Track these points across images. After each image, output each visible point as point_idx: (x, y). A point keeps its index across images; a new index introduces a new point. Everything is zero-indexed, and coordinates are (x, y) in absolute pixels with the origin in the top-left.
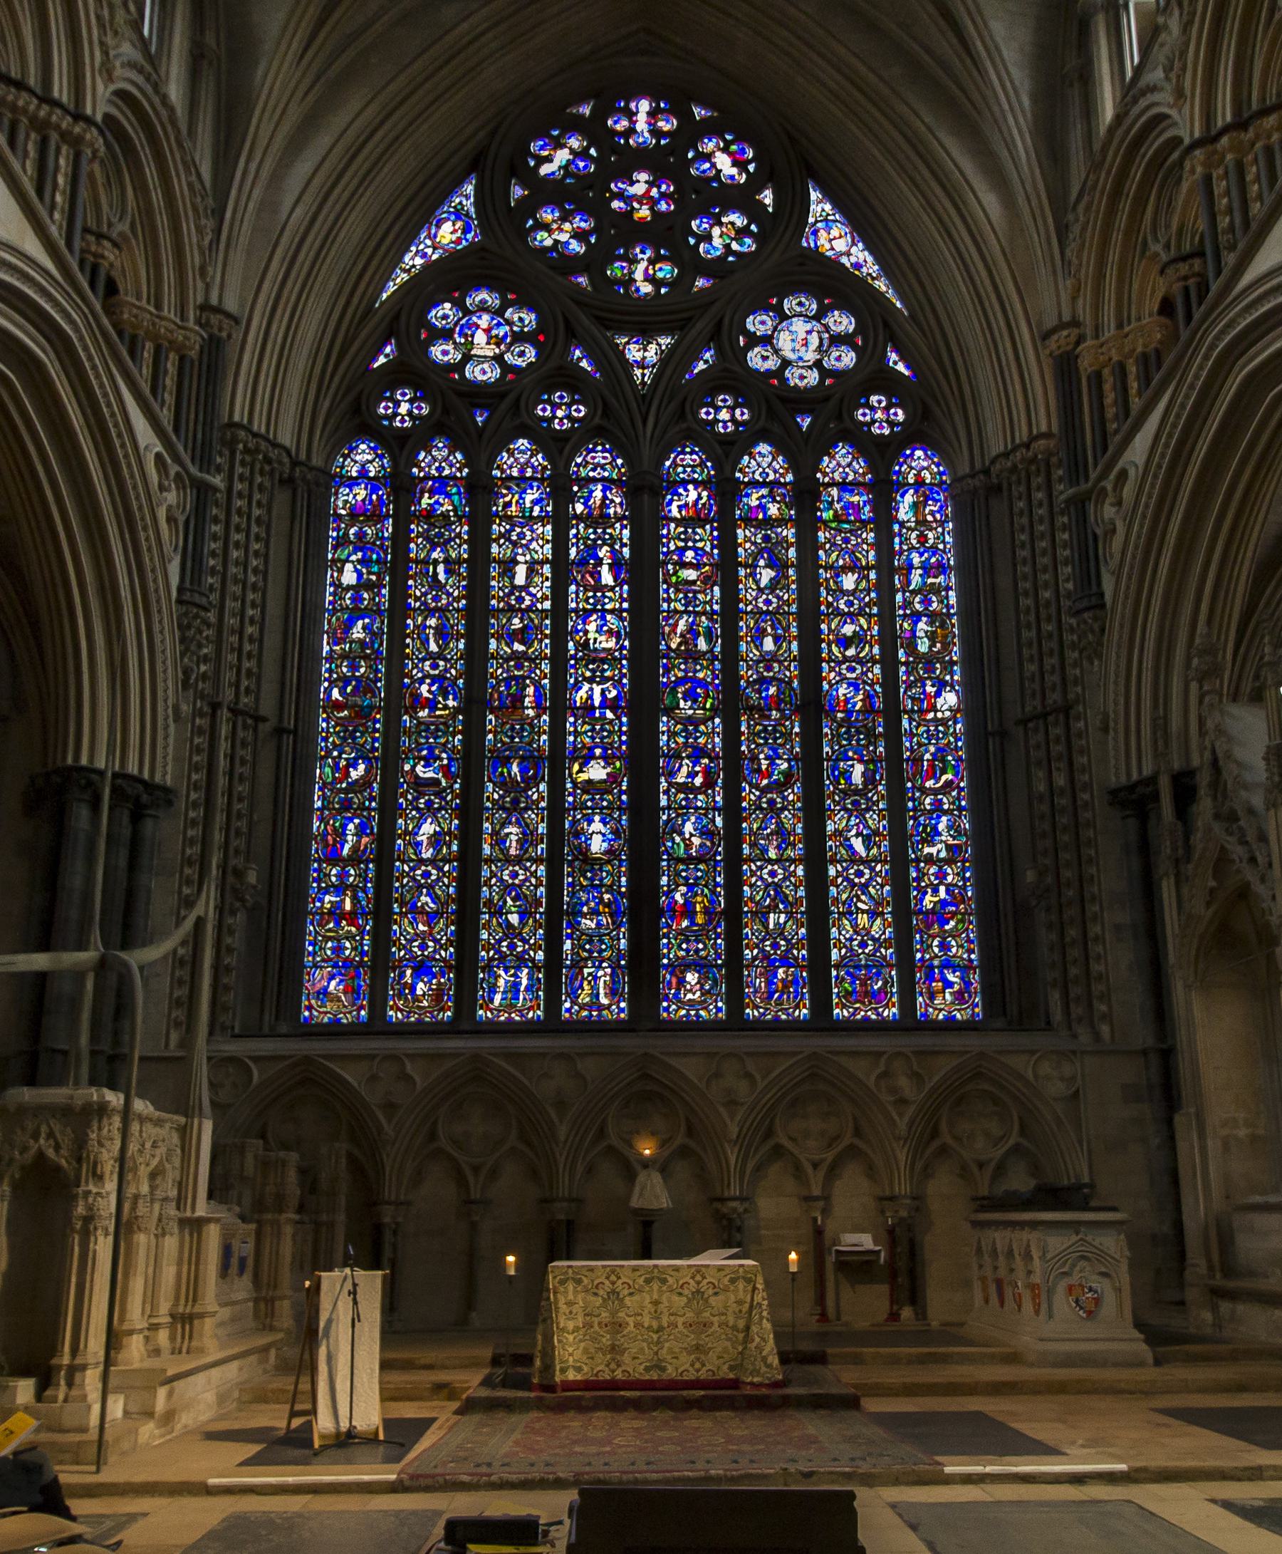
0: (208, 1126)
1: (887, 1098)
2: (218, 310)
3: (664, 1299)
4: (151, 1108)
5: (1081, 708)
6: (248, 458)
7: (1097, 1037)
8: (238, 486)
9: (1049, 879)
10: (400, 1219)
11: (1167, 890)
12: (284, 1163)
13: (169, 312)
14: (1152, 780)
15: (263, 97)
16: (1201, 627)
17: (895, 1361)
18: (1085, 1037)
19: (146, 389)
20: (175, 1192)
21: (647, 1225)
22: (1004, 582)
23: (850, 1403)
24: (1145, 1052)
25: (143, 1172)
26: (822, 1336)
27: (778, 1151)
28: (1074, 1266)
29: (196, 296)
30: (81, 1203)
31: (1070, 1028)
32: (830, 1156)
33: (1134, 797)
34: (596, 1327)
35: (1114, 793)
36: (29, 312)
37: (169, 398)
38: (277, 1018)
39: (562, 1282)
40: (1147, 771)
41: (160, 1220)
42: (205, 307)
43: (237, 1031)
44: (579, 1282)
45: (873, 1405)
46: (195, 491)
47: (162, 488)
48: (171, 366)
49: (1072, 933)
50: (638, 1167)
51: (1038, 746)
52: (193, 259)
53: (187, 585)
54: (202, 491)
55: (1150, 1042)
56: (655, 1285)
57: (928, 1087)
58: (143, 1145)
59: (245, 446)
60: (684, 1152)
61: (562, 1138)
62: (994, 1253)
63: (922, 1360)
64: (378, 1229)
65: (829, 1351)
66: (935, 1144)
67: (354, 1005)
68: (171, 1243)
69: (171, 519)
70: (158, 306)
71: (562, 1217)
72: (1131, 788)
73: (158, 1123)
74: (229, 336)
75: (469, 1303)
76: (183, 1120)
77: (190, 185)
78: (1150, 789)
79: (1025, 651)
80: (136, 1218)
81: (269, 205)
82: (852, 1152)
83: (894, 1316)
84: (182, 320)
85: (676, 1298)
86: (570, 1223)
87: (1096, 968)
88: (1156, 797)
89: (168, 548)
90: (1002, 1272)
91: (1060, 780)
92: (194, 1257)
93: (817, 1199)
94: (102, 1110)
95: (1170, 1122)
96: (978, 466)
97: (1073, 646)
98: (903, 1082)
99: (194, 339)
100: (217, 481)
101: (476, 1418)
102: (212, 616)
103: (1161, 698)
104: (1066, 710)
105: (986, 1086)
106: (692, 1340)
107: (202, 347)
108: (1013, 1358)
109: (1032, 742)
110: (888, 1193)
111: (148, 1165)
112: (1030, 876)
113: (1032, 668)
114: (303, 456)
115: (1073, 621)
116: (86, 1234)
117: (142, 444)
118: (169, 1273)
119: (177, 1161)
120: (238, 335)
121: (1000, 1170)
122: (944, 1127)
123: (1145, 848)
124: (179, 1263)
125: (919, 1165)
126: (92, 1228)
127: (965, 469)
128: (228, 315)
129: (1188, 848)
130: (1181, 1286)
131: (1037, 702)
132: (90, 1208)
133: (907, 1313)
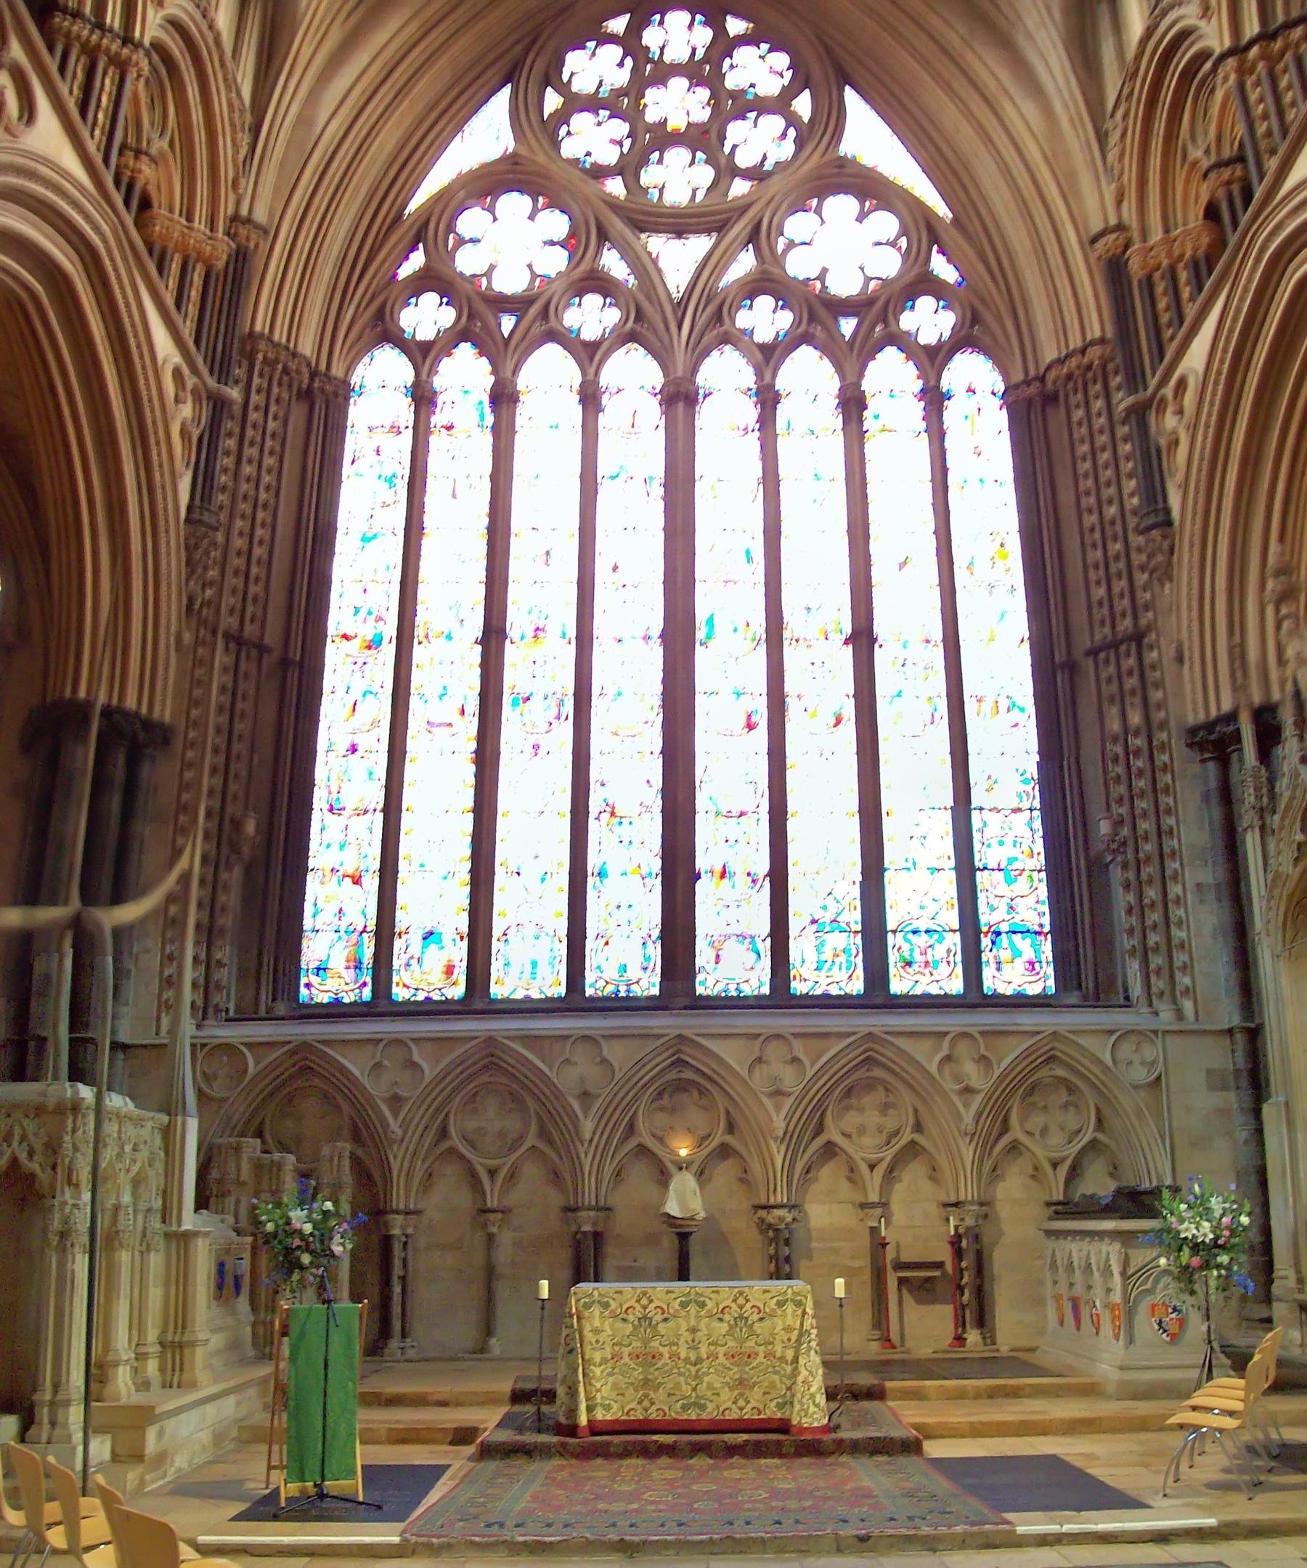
0: (193, 1125)
1: (951, 1086)
2: (249, 221)
3: (702, 1325)
4: (131, 1105)
5: (1153, 636)
6: (267, 369)
7: (1180, 1015)
8: (255, 398)
9: (1125, 831)
10: (410, 1231)
11: (1251, 843)
12: (279, 1166)
13: (200, 224)
14: (1232, 717)
15: (308, 18)
16: (1274, 546)
17: (960, 1395)
18: (1166, 1016)
19: (170, 300)
20: (160, 1202)
21: (684, 1237)
22: (1066, 497)
23: (911, 1447)
24: (1230, 1032)
25: (124, 1180)
26: (882, 1367)
27: (830, 1150)
28: (1157, 1281)
29: (226, 208)
30: (57, 1216)
31: (1150, 1005)
32: (889, 1155)
33: (1213, 737)
34: (626, 1359)
35: (1193, 731)
36: (69, 233)
37: (193, 310)
38: (274, 999)
39: (587, 1306)
40: (1227, 706)
41: (144, 1235)
42: (235, 218)
43: (231, 1014)
44: (606, 1305)
45: (934, 1449)
46: (211, 405)
47: (177, 400)
48: (197, 278)
49: (1152, 893)
50: (672, 1169)
51: (1109, 680)
52: (227, 171)
53: (197, 502)
54: (219, 405)
55: (1236, 1020)
56: (693, 1309)
57: (997, 1072)
58: (122, 1148)
59: (265, 357)
60: (724, 1151)
61: (587, 1136)
62: (1070, 1268)
63: (992, 1394)
64: (387, 1241)
65: (889, 1385)
66: (1005, 1140)
67: (356, 981)
68: (156, 1260)
69: (184, 433)
70: (190, 219)
71: (587, 1228)
72: (1210, 726)
73: (139, 1122)
74: (257, 246)
75: (488, 1331)
76: (165, 1119)
77: (230, 105)
78: (1231, 728)
79: (1093, 575)
80: (117, 1232)
81: (304, 120)
82: (912, 1150)
83: (960, 1340)
84: (211, 230)
85: (716, 1324)
86: (597, 1236)
87: (1178, 934)
88: (1237, 737)
89: (179, 463)
90: (1079, 1290)
91: (1135, 718)
92: (180, 1278)
93: (872, 1205)
94: (76, 1107)
95: (1257, 1113)
96: (1032, 373)
97: (1142, 568)
98: (970, 1070)
99: (221, 250)
100: (234, 393)
101: (491, 1466)
102: (220, 537)
103: (1236, 624)
104: (1138, 638)
105: (1061, 1072)
106: (735, 1373)
107: (229, 256)
108: (1090, 1391)
109: (1104, 675)
110: (953, 1199)
111: (128, 1171)
112: (1104, 828)
113: (1101, 592)
114: (323, 367)
115: (1141, 540)
116: (63, 1249)
117: (160, 358)
118: (155, 1295)
119: (160, 1166)
120: (264, 247)
121: (1075, 1172)
122: (1014, 1120)
123: (1226, 796)
124: (167, 1284)
125: (988, 1166)
126: (69, 1244)
127: (1018, 376)
128: (258, 226)
129: (1273, 796)
130: (1268, 1299)
131: (1107, 630)
132: (66, 1222)
133: (973, 1336)
